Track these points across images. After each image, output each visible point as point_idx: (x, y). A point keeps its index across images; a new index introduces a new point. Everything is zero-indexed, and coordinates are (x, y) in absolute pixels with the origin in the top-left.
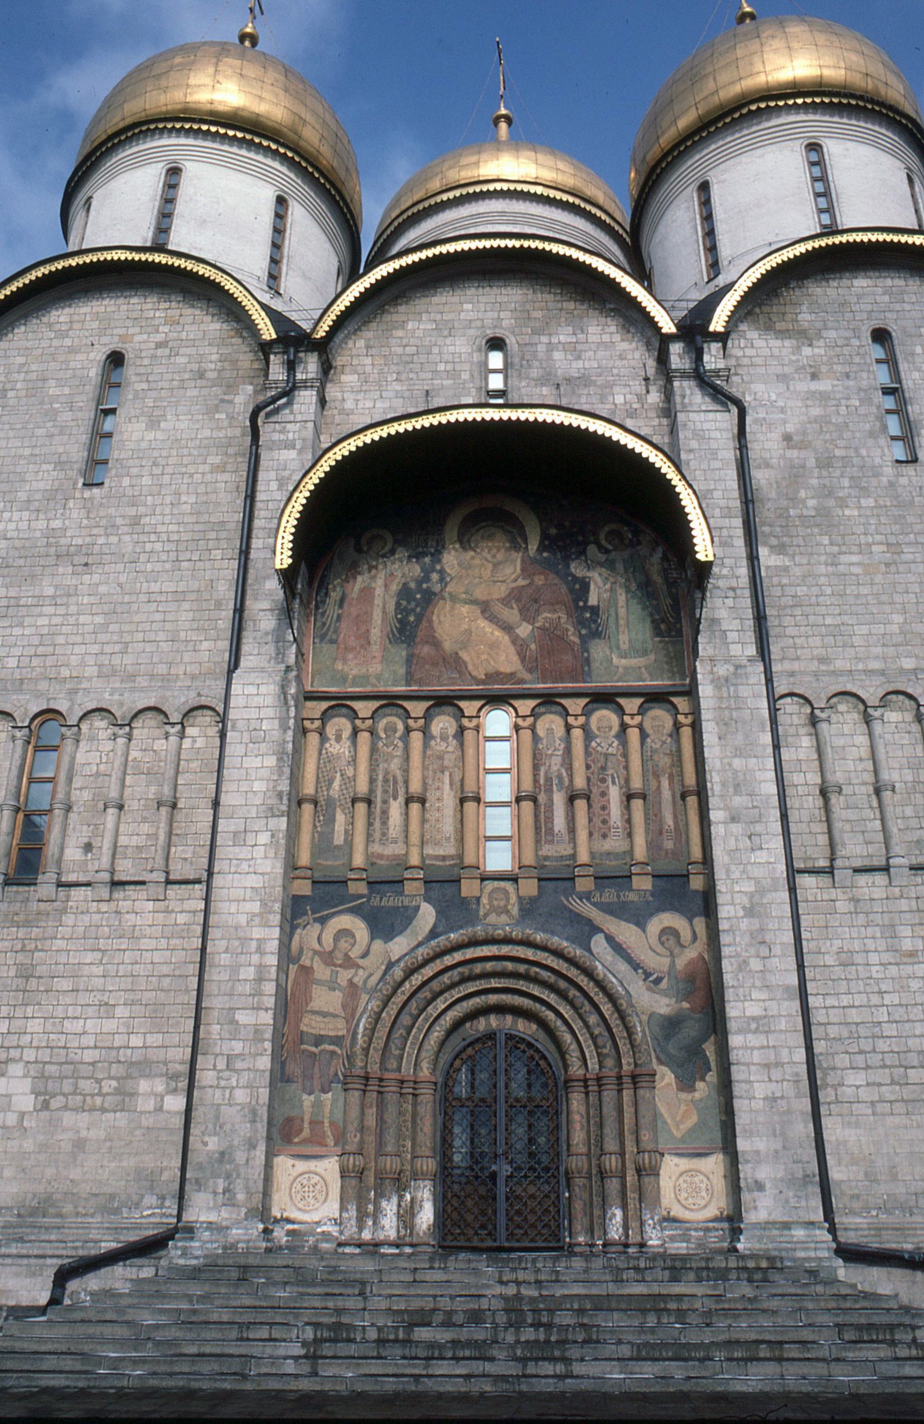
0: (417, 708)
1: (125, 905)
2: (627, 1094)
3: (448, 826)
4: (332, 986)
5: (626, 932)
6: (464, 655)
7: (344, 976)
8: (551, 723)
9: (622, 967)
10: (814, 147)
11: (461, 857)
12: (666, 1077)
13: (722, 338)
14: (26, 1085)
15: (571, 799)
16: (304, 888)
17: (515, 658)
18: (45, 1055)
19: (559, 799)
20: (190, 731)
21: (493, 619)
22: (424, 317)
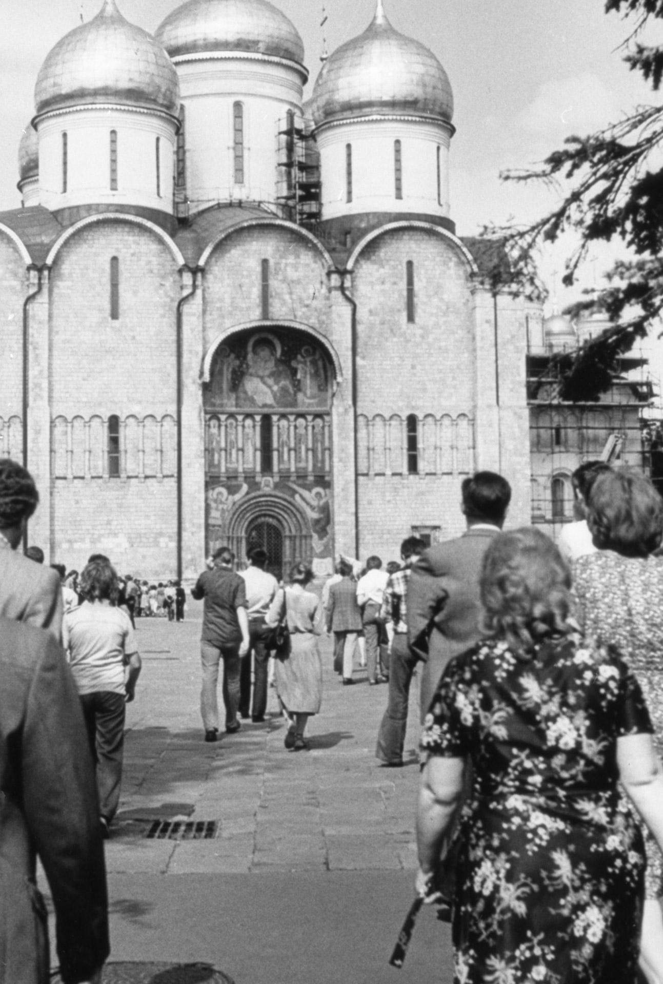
0: (240, 418)
1: (149, 484)
2: (303, 541)
3: (251, 458)
4: (217, 509)
5: (306, 494)
6: (255, 397)
7: (220, 507)
8: (284, 423)
9: (303, 504)
10: (398, 142)
11: (255, 468)
12: (315, 536)
13: (351, 272)
14: (126, 540)
15: (290, 450)
16: (208, 479)
17: (272, 399)
18: (130, 531)
19: (286, 449)
20: (164, 423)
21: (264, 383)
22: (238, 248)
